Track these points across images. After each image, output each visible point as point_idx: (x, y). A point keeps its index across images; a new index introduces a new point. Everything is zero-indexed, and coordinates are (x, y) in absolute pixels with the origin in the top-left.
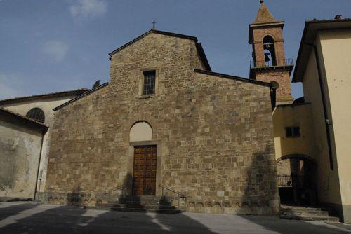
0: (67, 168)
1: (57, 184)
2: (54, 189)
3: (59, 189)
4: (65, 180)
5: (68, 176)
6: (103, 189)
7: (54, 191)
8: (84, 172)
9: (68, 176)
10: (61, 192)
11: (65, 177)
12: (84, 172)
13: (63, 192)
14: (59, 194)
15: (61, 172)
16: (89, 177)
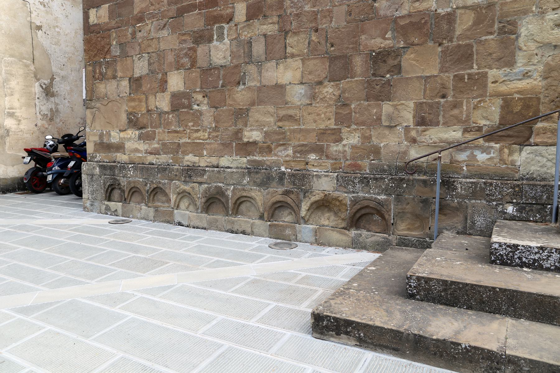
0: (168, 40)
1: (133, 122)
2: (119, 147)
3: (142, 146)
4: (163, 102)
5: (176, 82)
6: (391, 143)
7: (122, 157)
8: (259, 49)
9: (176, 82)
10: (151, 159)
11: (163, 85)
12: (259, 49)
13: (164, 159)
14: (145, 169)
15: (140, 67)
16: (286, 74)
